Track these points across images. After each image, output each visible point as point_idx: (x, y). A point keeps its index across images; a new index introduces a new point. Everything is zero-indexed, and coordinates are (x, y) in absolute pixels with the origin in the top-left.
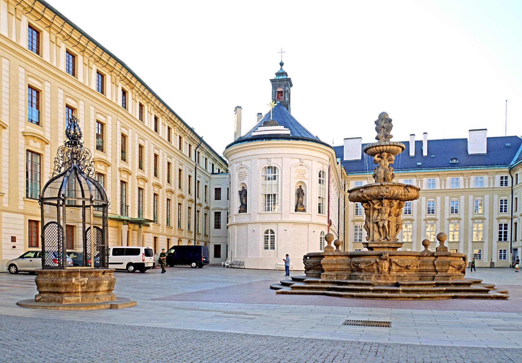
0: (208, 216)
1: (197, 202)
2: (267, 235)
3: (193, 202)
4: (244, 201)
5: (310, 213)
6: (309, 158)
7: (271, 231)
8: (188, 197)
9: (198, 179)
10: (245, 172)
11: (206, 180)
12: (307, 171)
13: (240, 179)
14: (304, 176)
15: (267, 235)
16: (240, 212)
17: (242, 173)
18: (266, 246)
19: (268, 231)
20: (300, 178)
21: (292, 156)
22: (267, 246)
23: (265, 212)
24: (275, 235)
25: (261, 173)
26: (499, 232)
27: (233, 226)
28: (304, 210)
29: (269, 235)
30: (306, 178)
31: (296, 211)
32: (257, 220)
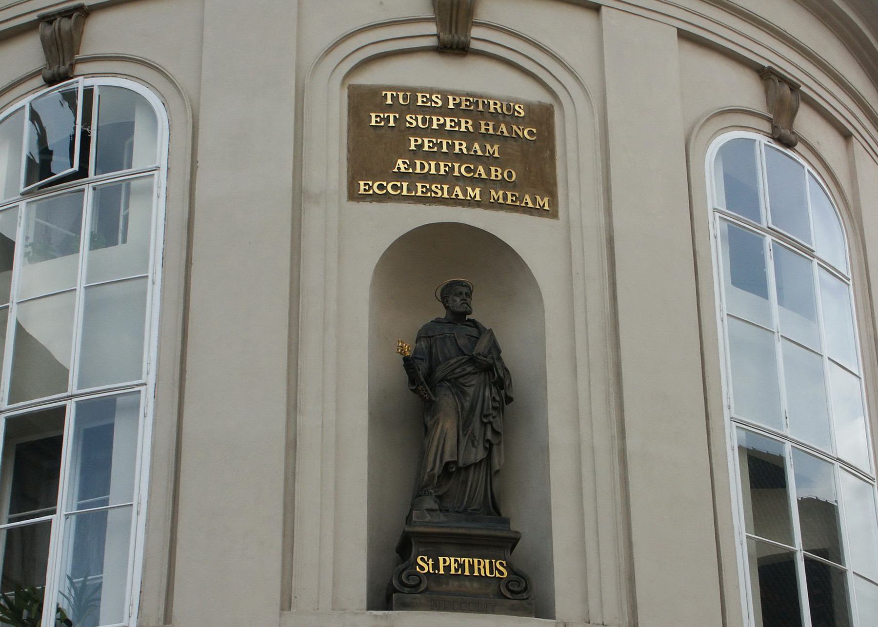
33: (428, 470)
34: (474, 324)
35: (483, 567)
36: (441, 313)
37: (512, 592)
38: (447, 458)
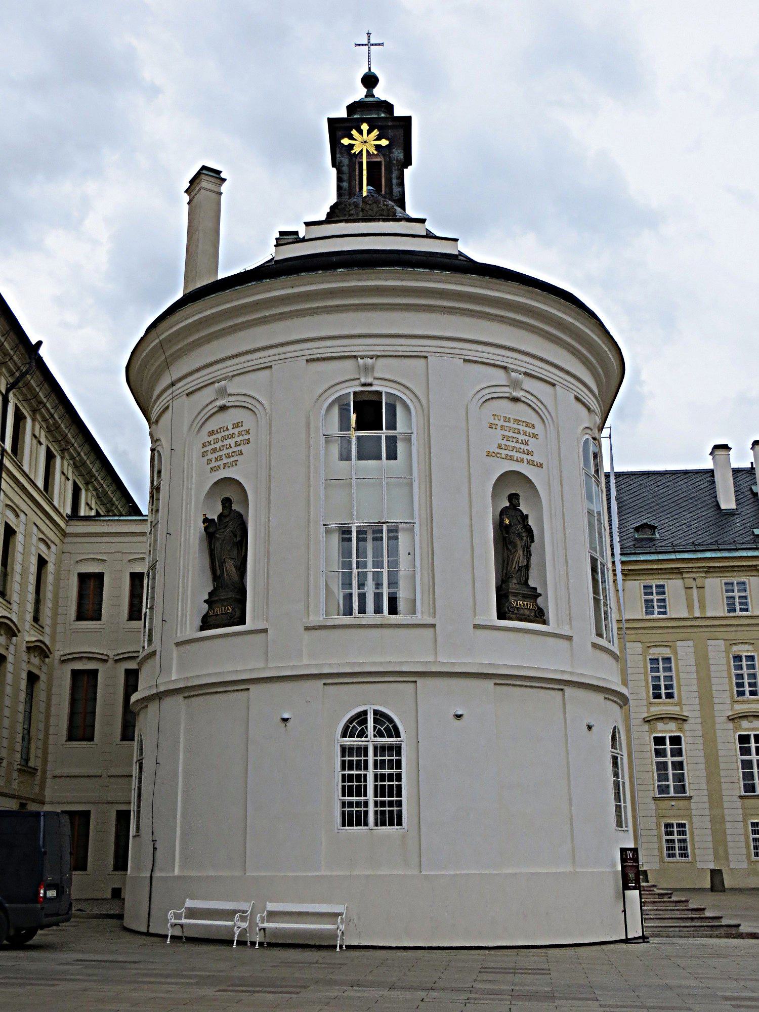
0: (42, 685)
2: (355, 741)
4: (230, 567)
5: (566, 631)
6: (543, 374)
7: (380, 717)
10: (236, 425)
12: (539, 429)
13: (213, 464)
15: (355, 741)
16: (206, 624)
17: (219, 436)
18: (351, 804)
19: (365, 721)
20: (511, 458)
21: (473, 352)
22: (358, 804)
24: (405, 741)
27: (168, 702)
28: (540, 616)
29: (371, 740)
30: (535, 458)
31: (501, 615)
32: (305, 661)
33: (514, 567)
34: (520, 511)
35: (530, 604)
36: (508, 504)
37: (539, 615)
38: (520, 565)
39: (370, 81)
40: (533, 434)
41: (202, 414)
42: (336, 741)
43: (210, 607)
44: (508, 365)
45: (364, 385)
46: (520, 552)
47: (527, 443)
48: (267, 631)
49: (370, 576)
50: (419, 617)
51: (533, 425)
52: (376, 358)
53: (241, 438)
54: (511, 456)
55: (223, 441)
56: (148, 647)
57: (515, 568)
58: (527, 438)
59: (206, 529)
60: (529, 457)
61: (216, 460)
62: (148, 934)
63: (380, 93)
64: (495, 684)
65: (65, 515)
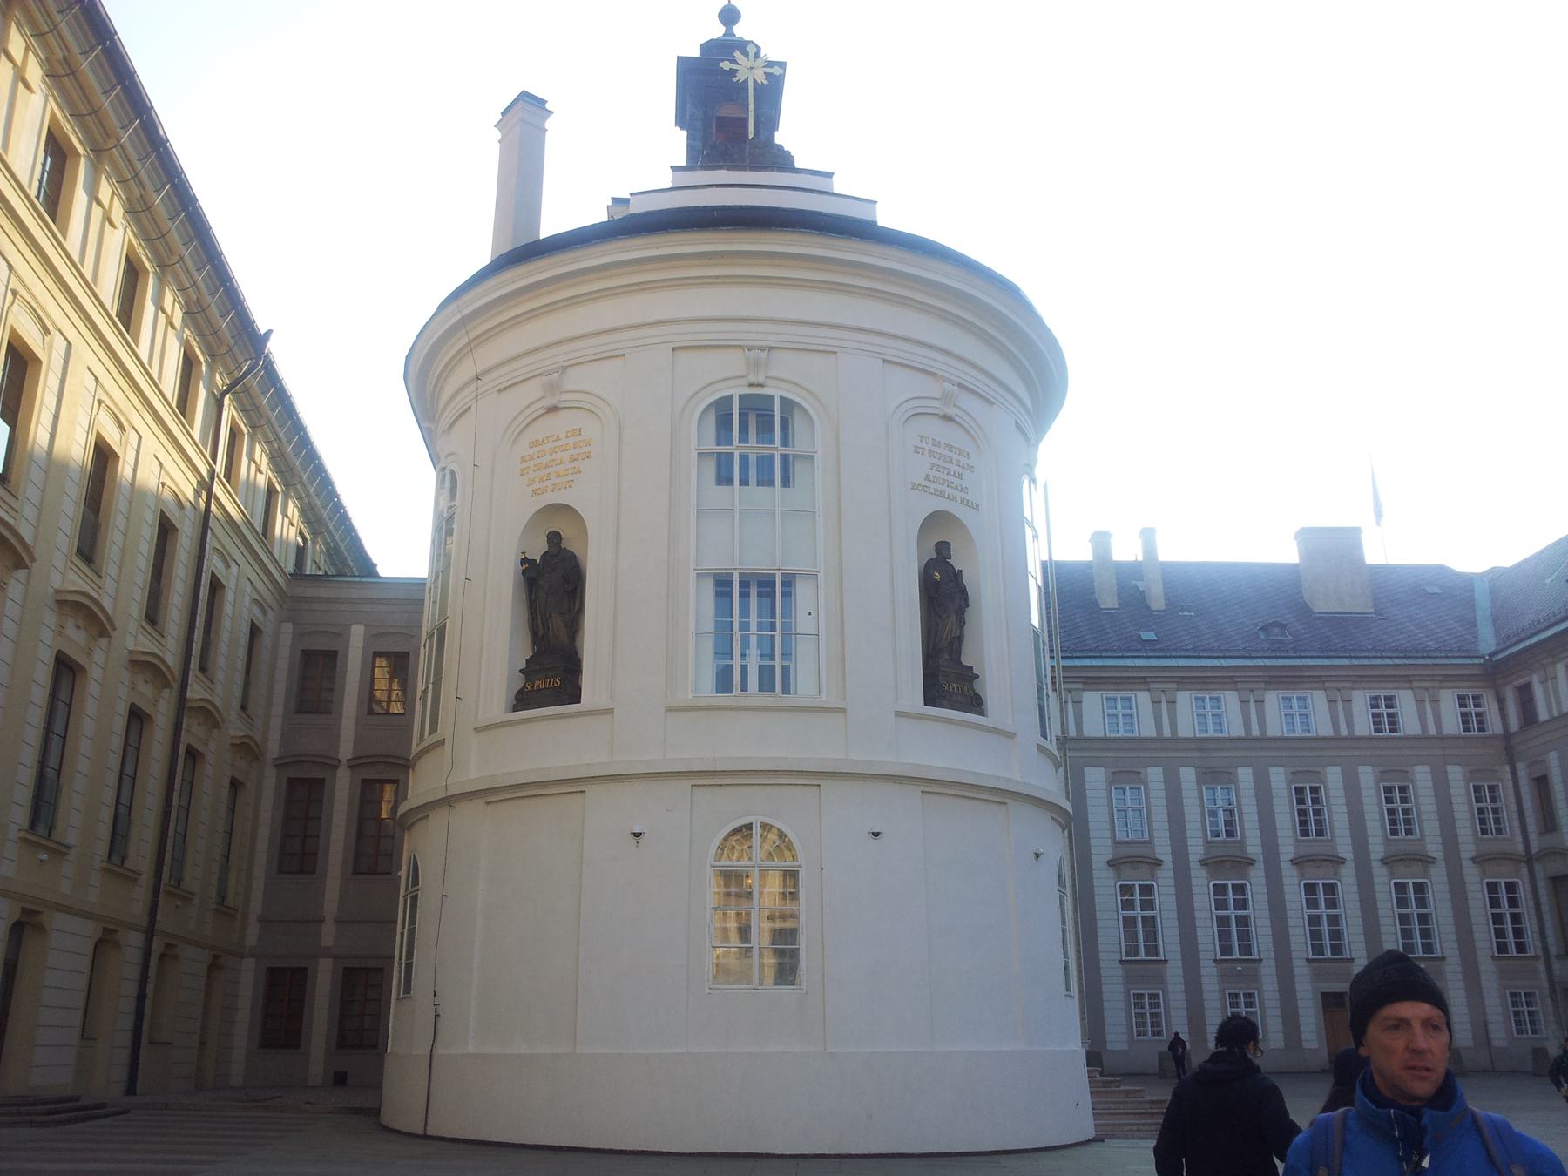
1: (195, 691)
3: (167, 685)
4: (557, 623)
8: (132, 637)
9: (213, 563)
11: (258, 593)
14: (957, 481)
16: (523, 700)
20: (941, 494)
23: (724, 699)
25: (698, 436)
26: (1400, 915)
27: (464, 811)
28: (975, 704)
31: (930, 701)
33: (944, 637)
39: (729, 16)
40: (968, 465)
41: (521, 418)
42: (708, 866)
43: (528, 680)
44: (940, 373)
45: (751, 385)
46: (953, 618)
47: (960, 477)
48: (613, 712)
49: (753, 640)
50: (824, 698)
51: (968, 454)
52: (769, 351)
53: (577, 451)
54: (941, 492)
55: (551, 455)
56: (429, 735)
57: (946, 638)
58: (958, 470)
59: (524, 572)
60: (962, 495)
61: (541, 480)
62: (425, 1137)
63: (740, 31)
64: (922, 792)
65: (287, 571)
